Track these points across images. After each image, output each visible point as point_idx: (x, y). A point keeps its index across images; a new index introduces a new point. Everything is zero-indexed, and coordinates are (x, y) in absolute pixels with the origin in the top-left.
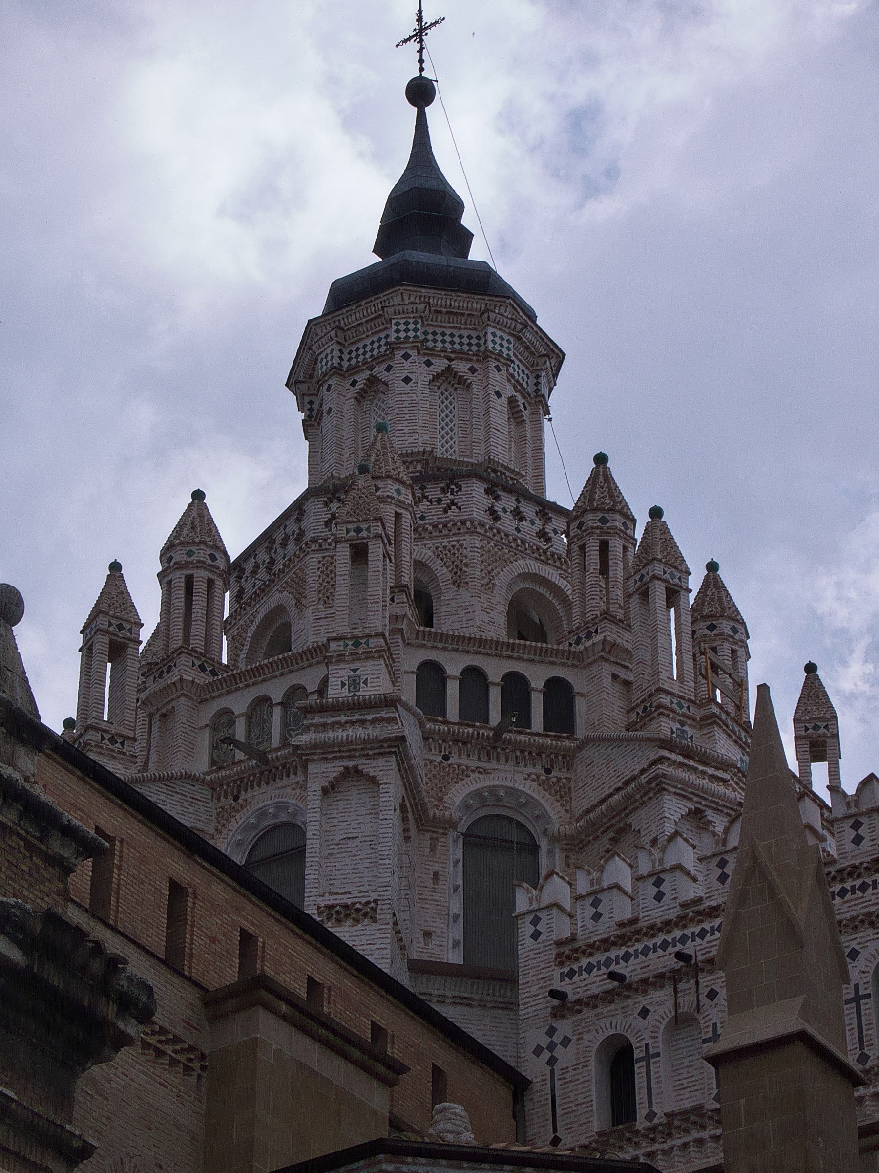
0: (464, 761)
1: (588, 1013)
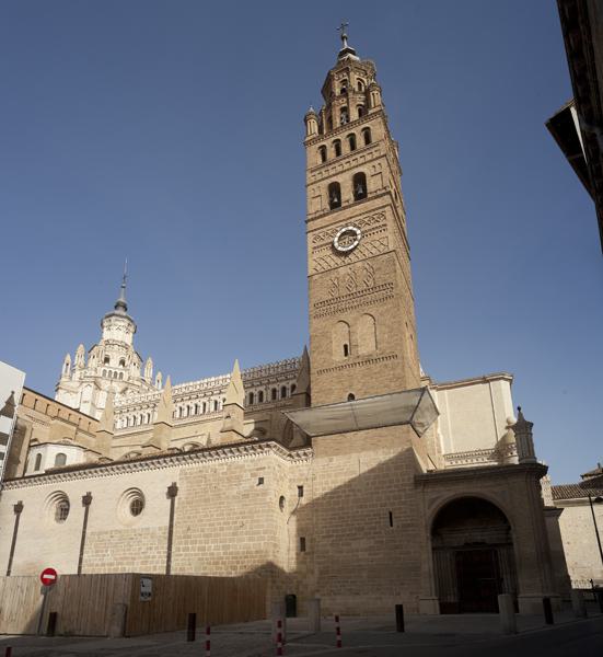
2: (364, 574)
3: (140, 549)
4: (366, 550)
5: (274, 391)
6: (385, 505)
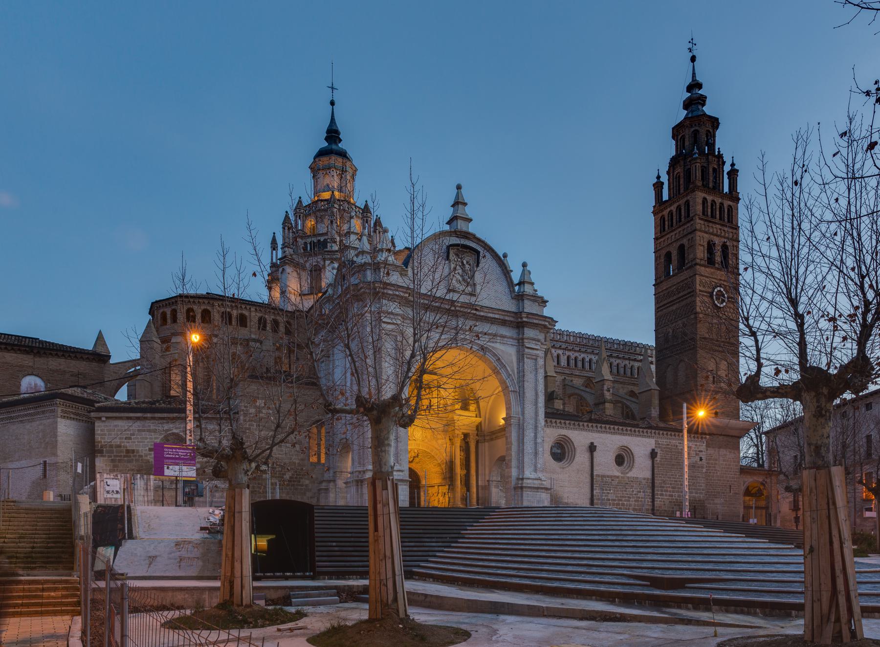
3: (633, 491)
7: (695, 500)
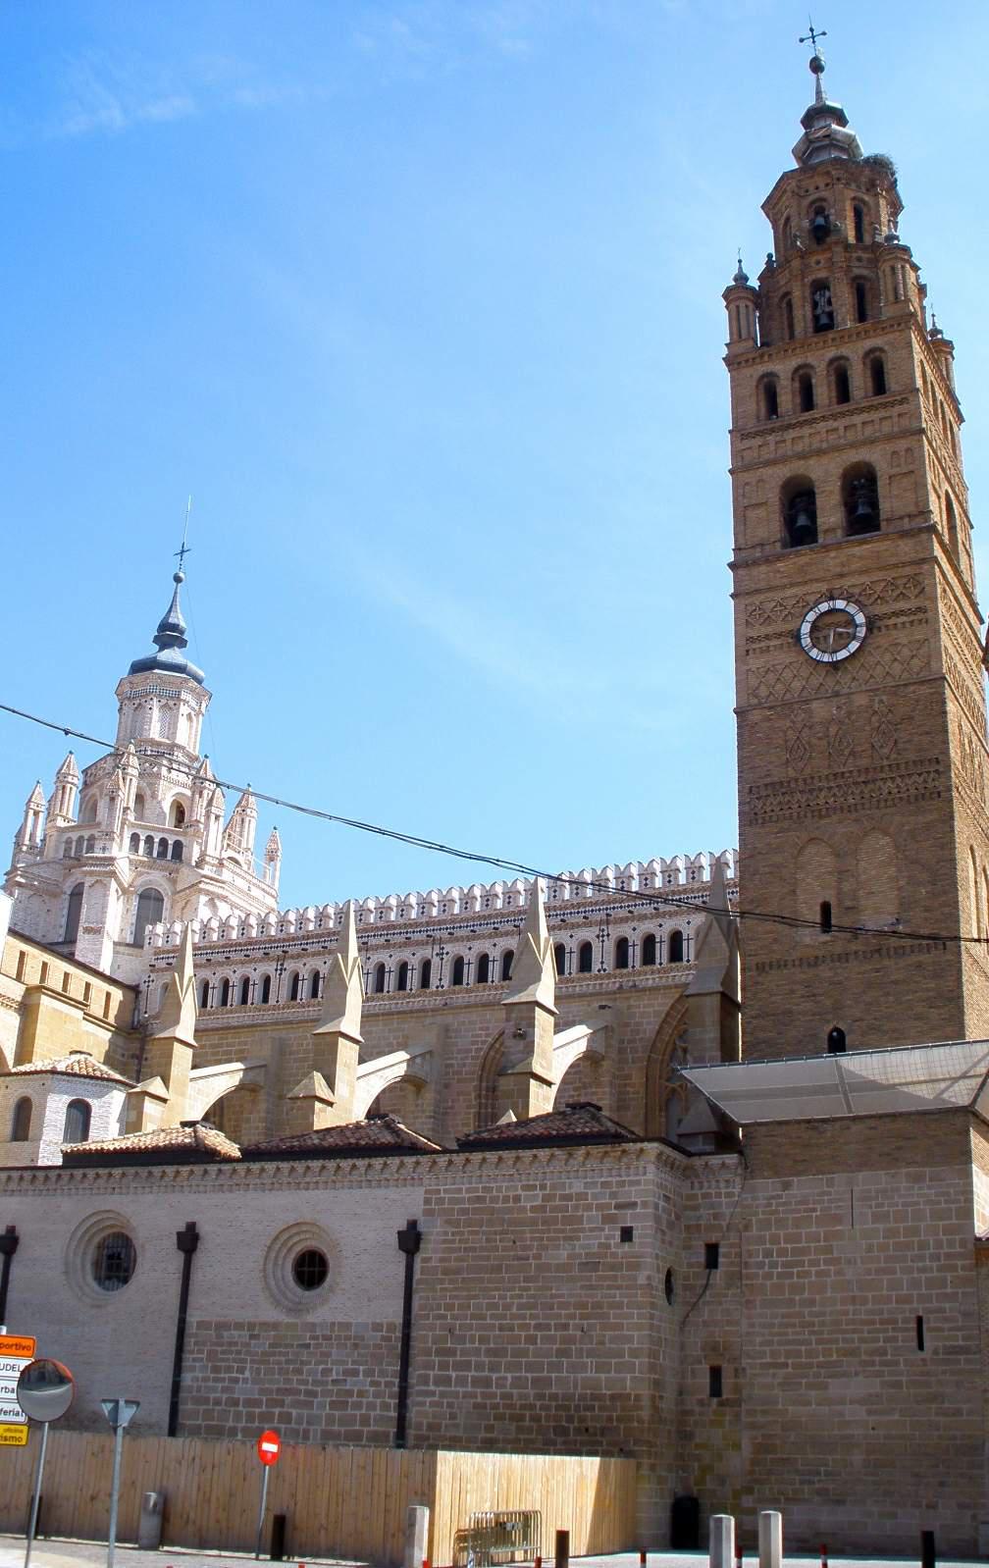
0: (143, 870)
1: (160, 973)
2: (857, 1458)
3: (326, 1372)
4: (861, 1402)
5: (622, 945)
6: (908, 1300)
7: (594, 1397)
